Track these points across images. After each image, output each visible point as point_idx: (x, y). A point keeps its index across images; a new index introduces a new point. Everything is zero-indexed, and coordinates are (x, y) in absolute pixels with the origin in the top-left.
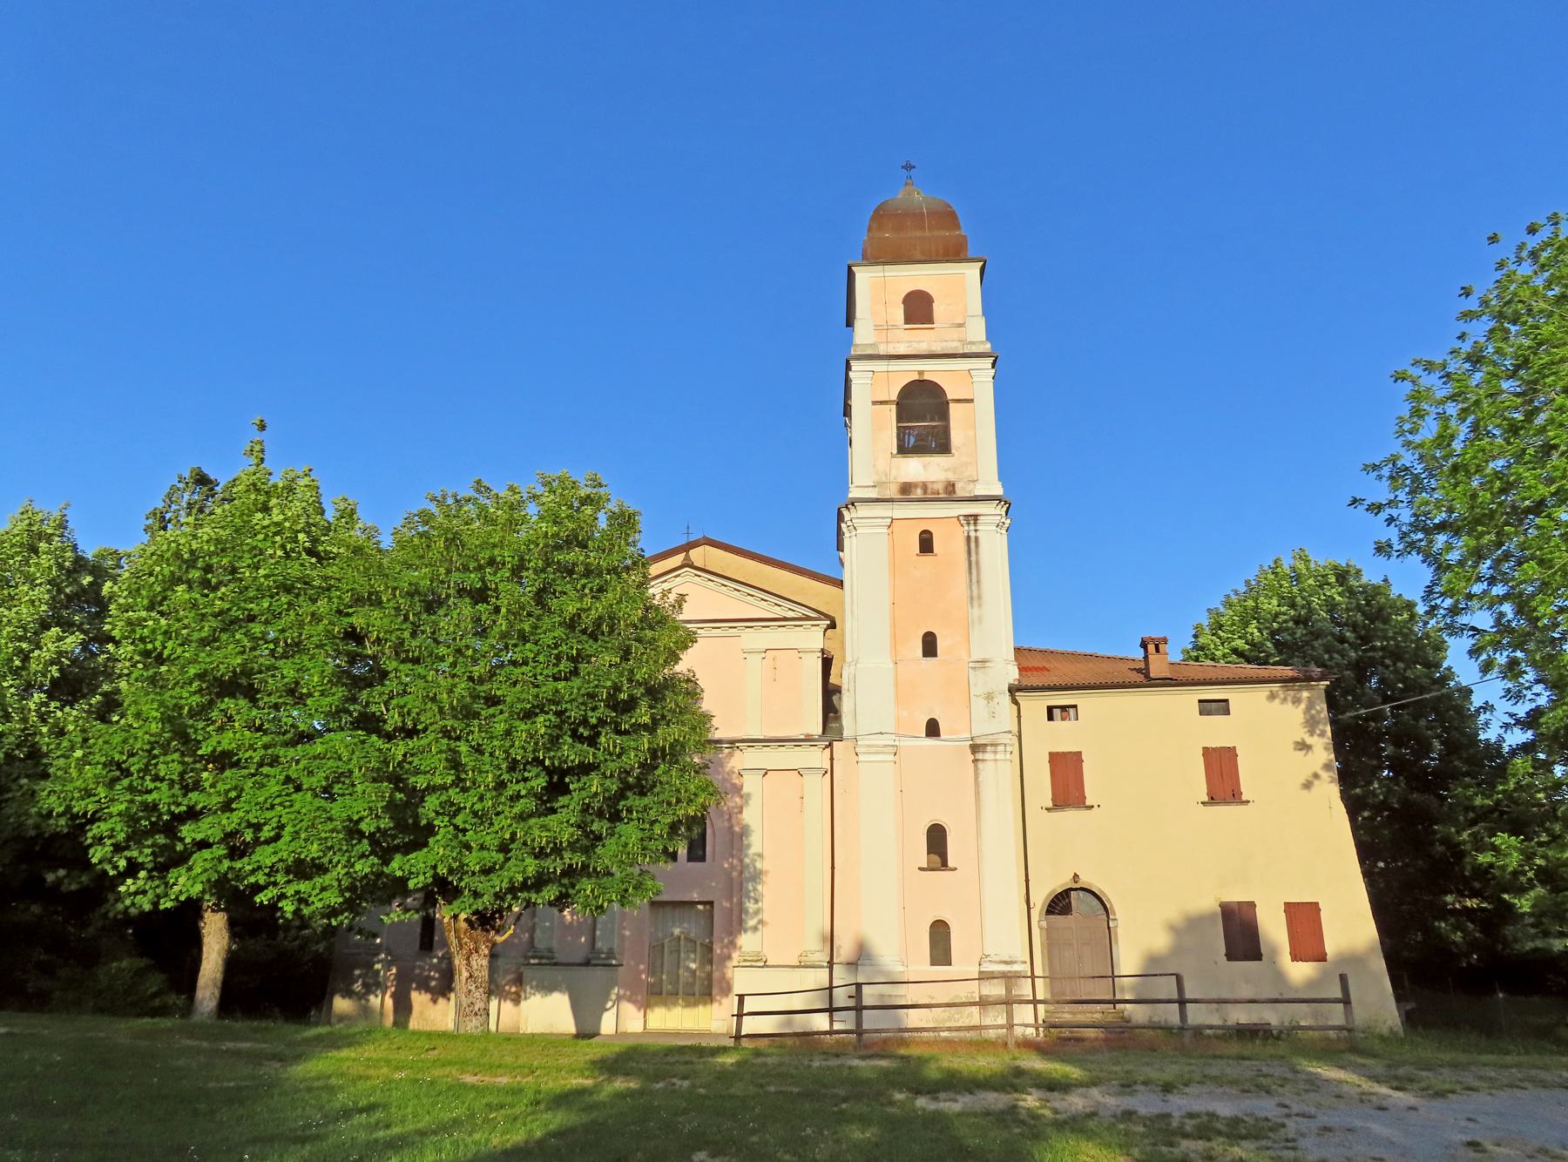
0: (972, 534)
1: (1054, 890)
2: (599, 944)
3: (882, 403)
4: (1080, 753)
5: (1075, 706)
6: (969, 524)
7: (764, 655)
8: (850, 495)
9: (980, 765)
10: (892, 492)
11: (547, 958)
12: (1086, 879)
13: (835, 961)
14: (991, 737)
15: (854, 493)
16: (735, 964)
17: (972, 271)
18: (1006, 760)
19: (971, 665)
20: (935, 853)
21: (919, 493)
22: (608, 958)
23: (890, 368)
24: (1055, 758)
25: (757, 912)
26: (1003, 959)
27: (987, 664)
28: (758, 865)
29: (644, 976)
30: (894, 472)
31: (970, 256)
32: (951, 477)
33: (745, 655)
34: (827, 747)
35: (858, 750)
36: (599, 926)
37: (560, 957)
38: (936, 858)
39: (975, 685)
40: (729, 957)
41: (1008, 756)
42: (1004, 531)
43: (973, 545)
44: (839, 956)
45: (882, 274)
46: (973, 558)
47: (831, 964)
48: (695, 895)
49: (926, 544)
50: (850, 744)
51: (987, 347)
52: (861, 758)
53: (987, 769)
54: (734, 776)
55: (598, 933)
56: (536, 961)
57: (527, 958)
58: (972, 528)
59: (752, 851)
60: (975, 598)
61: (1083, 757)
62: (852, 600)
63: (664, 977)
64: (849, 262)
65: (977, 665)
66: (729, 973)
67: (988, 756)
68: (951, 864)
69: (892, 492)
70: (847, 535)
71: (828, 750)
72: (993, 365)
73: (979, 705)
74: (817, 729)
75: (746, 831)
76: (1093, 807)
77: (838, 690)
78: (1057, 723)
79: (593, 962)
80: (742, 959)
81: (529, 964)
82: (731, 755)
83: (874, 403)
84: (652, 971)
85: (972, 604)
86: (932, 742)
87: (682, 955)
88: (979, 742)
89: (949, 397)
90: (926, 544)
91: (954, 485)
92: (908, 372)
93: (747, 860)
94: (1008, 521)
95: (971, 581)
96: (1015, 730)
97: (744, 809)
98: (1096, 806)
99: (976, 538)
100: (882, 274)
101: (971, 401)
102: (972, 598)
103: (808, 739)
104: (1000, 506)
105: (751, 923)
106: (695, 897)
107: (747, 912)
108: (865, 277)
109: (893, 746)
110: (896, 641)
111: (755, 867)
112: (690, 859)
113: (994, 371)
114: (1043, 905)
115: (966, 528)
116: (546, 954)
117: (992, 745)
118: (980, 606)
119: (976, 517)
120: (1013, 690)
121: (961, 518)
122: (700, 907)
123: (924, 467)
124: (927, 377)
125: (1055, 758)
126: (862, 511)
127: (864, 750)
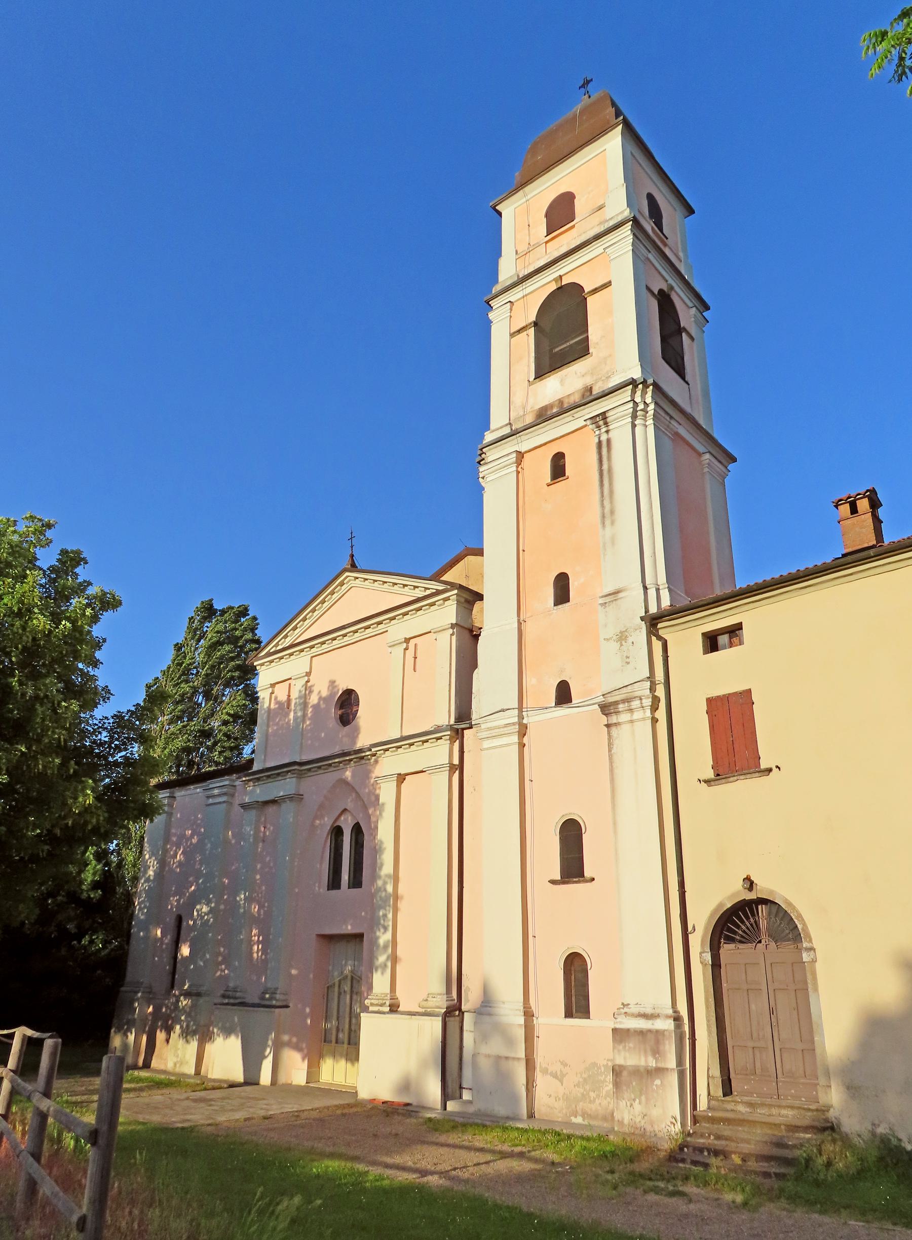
0: (604, 438)
1: (721, 905)
3: (519, 331)
9: (614, 730)
12: (766, 885)
14: (624, 690)
22: (271, 999)
26: (642, 1011)
27: (620, 595)
32: (588, 381)
44: (467, 1001)
46: (605, 467)
48: (349, 927)
49: (558, 468)
53: (622, 734)
60: (607, 515)
64: (491, 204)
65: (608, 599)
67: (624, 717)
68: (587, 874)
76: (770, 770)
85: (603, 523)
90: (558, 468)
98: (774, 768)
102: (603, 517)
114: (706, 928)
115: (597, 433)
117: (624, 701)
118: (613, 523)
119: (603, 416)
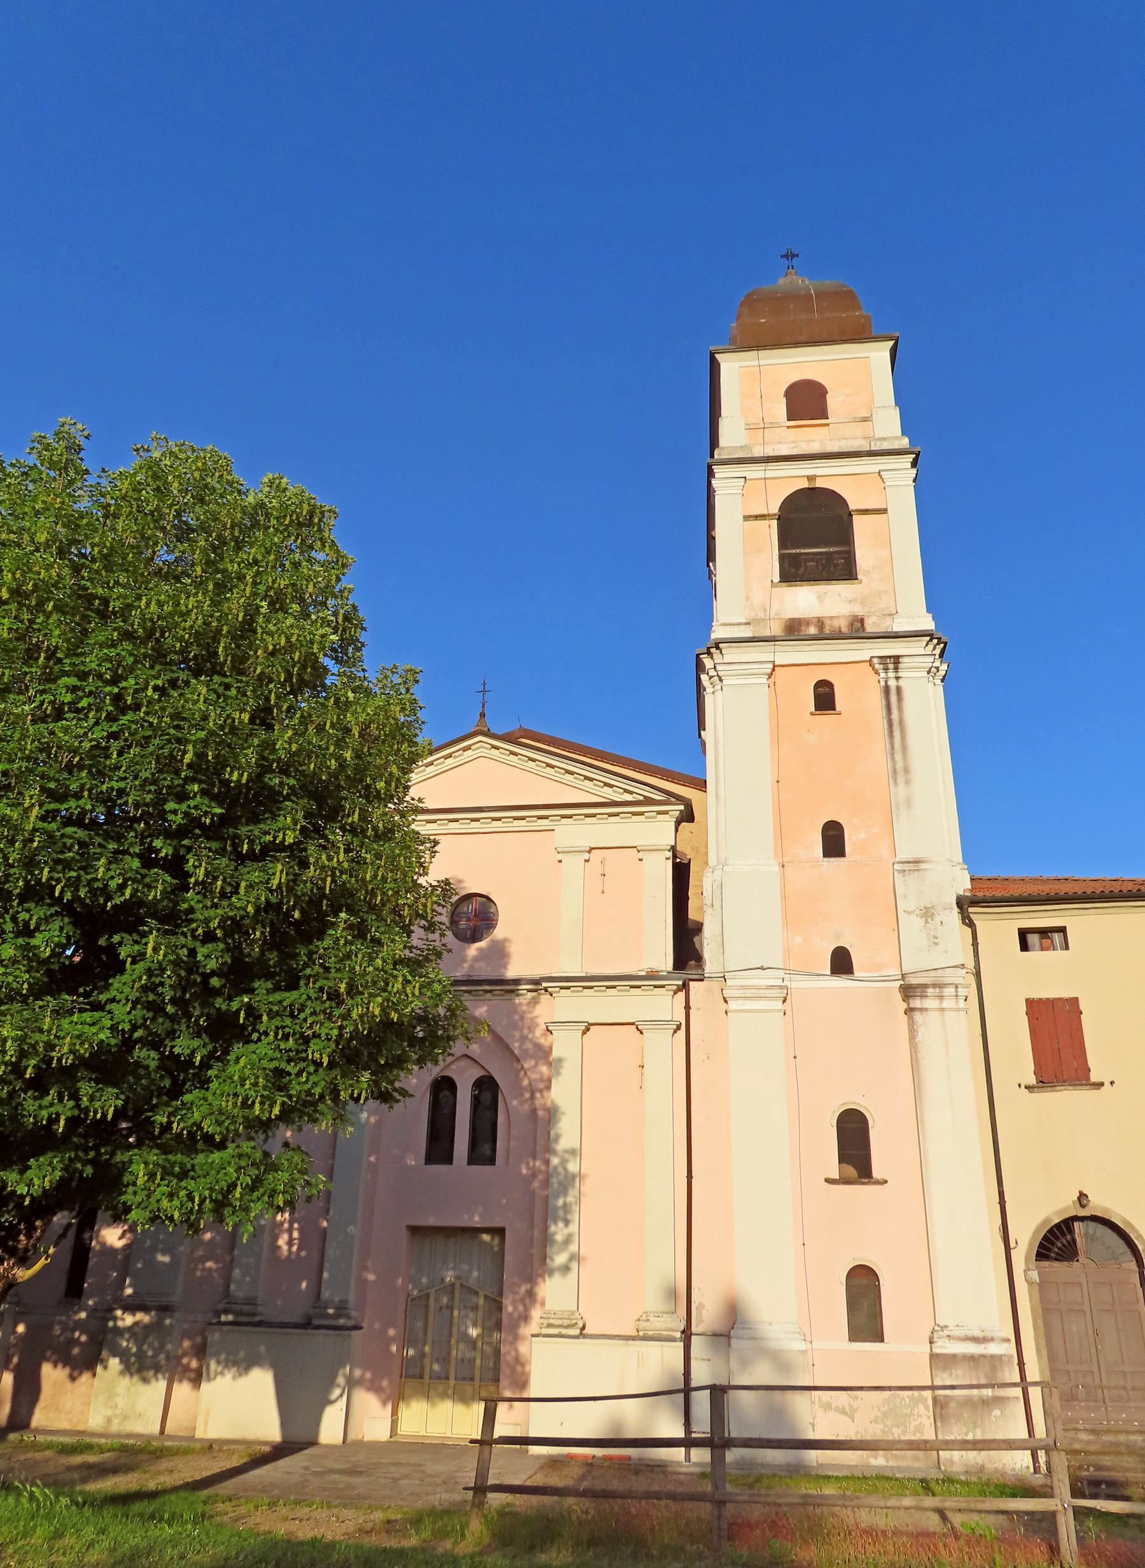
0: (892, 683)
1: (1047, 1220)
2: (326, 1294)
3: (757, 517)
4: (1075, 1001)
5: (1062, 930)
6: (886, 669)
7: (587, 856)
8: (714, 636)
9: (918, 1016)
10: (776, 629)
11: (248, 1314)
12: (1101, 1202)
13: (694, 1329)
14: (933, 973)
15: (718, 633)
16: (536, 1331)
17: (878, 354)
18: (958, 1010)
19: (897, 867)
20: (848, 1163)
21: (812, 630)
22: (336, 1316)
23: (769, 474)
24: (1034, 1007)
25: (568, 1240)
26: (970, 1334)
27: (923, 866)
28: (572, 1167)
29: (394, 1348)
30: (775, 605)
31: (874, 334)
32: (858, 610)
33: (560, 857)
34: (679, 989)
35: (727, 993)
36: (327, 1265)
37: (266, 1312)
38: (851, 1171)
39: (905, 896)
40: (526, 1318)
41: (962, 1004)
42: (938, 682)
43: (894, 698)
44: (700, 1321)
45: (756, 363)
46: (895, 716)
47: (687, 1335)
48: (477, 1219)
49: (825, 699)
50: (715, 985)
51: (905, 442)
52: (732, 1005)
53: (930, 1024)
54: (538, 1033)
55: (326, 1275)
56: (230, 1318)
57: (218, 1314)
58: (891, 674)
59: (562, 1145)
60: (900, 771)
61: (1082, 1007)
62: (717, 778)
63: (427, 1349)
64: (712, 348)
65: (907, 867)
66: (523, 1348)
67: (929, 1003)
68: (876, 1174)
69: (776, 629)
70: (709, 690)
71: (682, 995)
72: (914, 464)
73: (911, 925)
74: (666, 962)
75: (552, 1114)
76: (1102, 1084)
77: (698, 928)
78: (1034, 955)
79: (316, 1322)
80: (545, 1322)
81: (220, 1323)
82: (535, 1002)
83: (747, 518)
84: (407, 1340)
85: (895, 780)
86: (841, 982)
87: (456, 1313)
88: (913, 981)
89: (852, 506)
90: (825, 699)
91: (862, 621)
92: (793, 479)
93: (555, 1161)
94: (944, 667)
95: (892, 748)
96: (971, 964)
97: (553, 1081)
98: (1107, 1084)
99: (899, 689)
100: (756, 363)
101: (884, 511)
102: (895, 772)
103: (652, 976)
104: (931, 647)
105: (560, 1259)
106: (477, 1221)
107: (553, 1241)
108: (732, 367)
109: (781, 987)
110: (781, 834)
111: (565, 1169)
112: (473, 1160)
113: (914, 471)
114: (1031, 1245)
115: (883, 675)
116: (246, 1308)
117: (935, 986)
118: (908, 782)
119: (896, 659)
120: (963, 904)
121: (875, 661)
122: (486, 1237)
123: (819, 597)
124: (819, 483)
125: (1034, 1007)
126: (731, 654)
127: (735, 993)
